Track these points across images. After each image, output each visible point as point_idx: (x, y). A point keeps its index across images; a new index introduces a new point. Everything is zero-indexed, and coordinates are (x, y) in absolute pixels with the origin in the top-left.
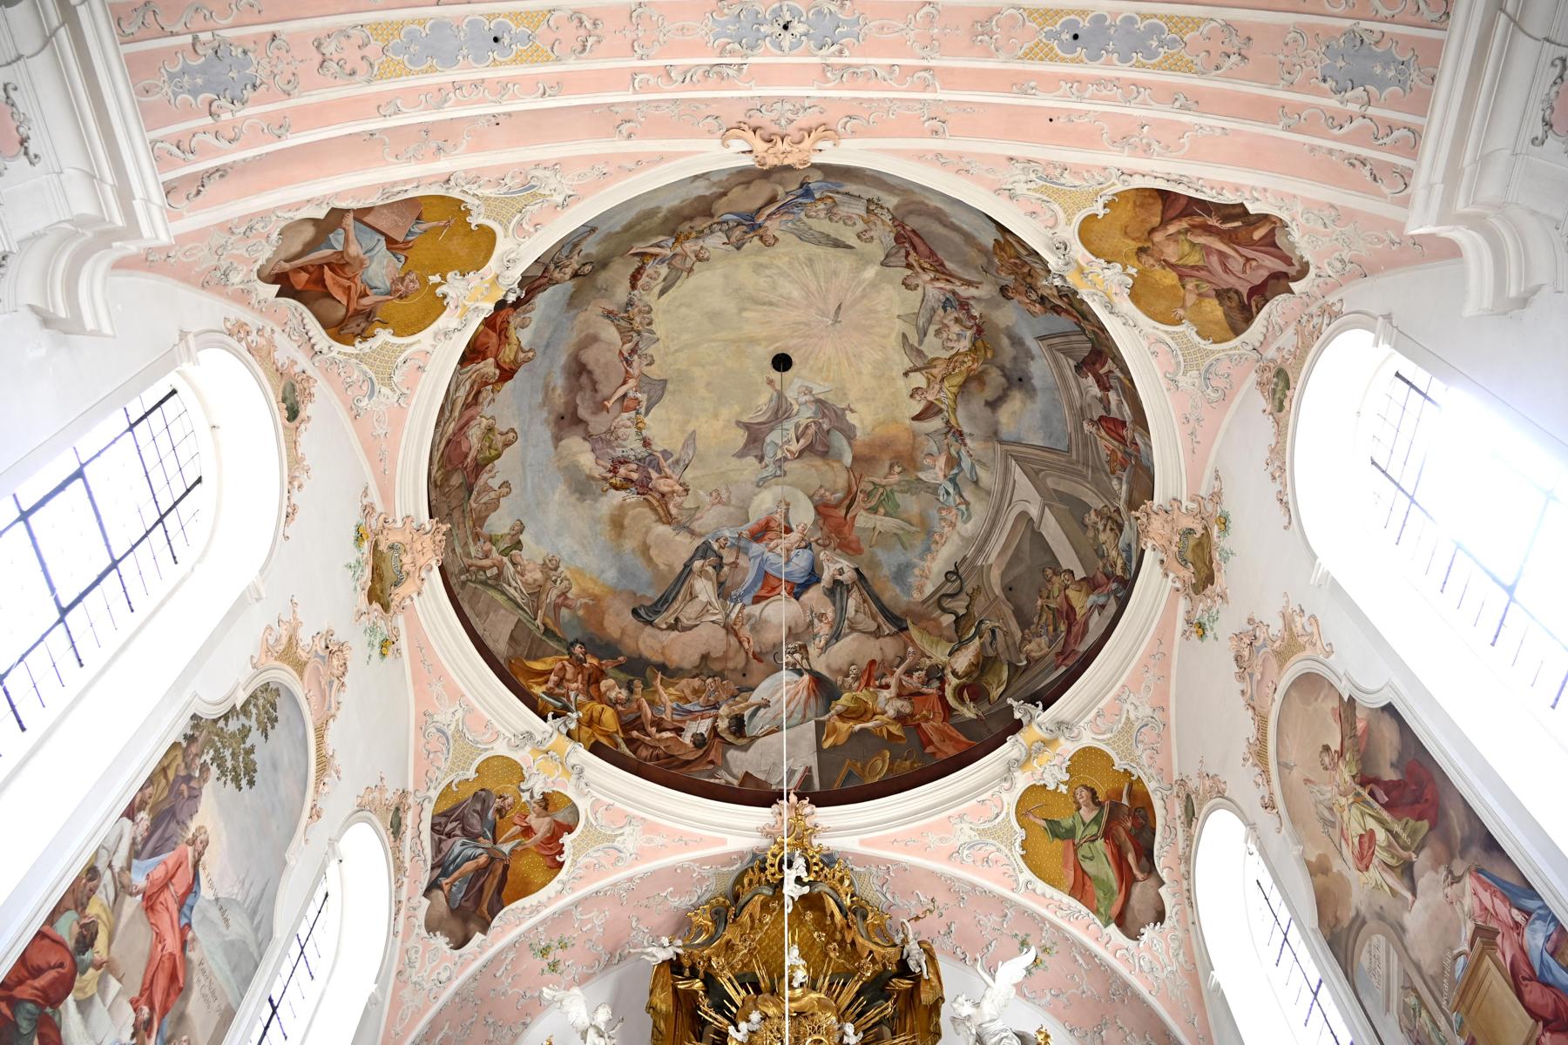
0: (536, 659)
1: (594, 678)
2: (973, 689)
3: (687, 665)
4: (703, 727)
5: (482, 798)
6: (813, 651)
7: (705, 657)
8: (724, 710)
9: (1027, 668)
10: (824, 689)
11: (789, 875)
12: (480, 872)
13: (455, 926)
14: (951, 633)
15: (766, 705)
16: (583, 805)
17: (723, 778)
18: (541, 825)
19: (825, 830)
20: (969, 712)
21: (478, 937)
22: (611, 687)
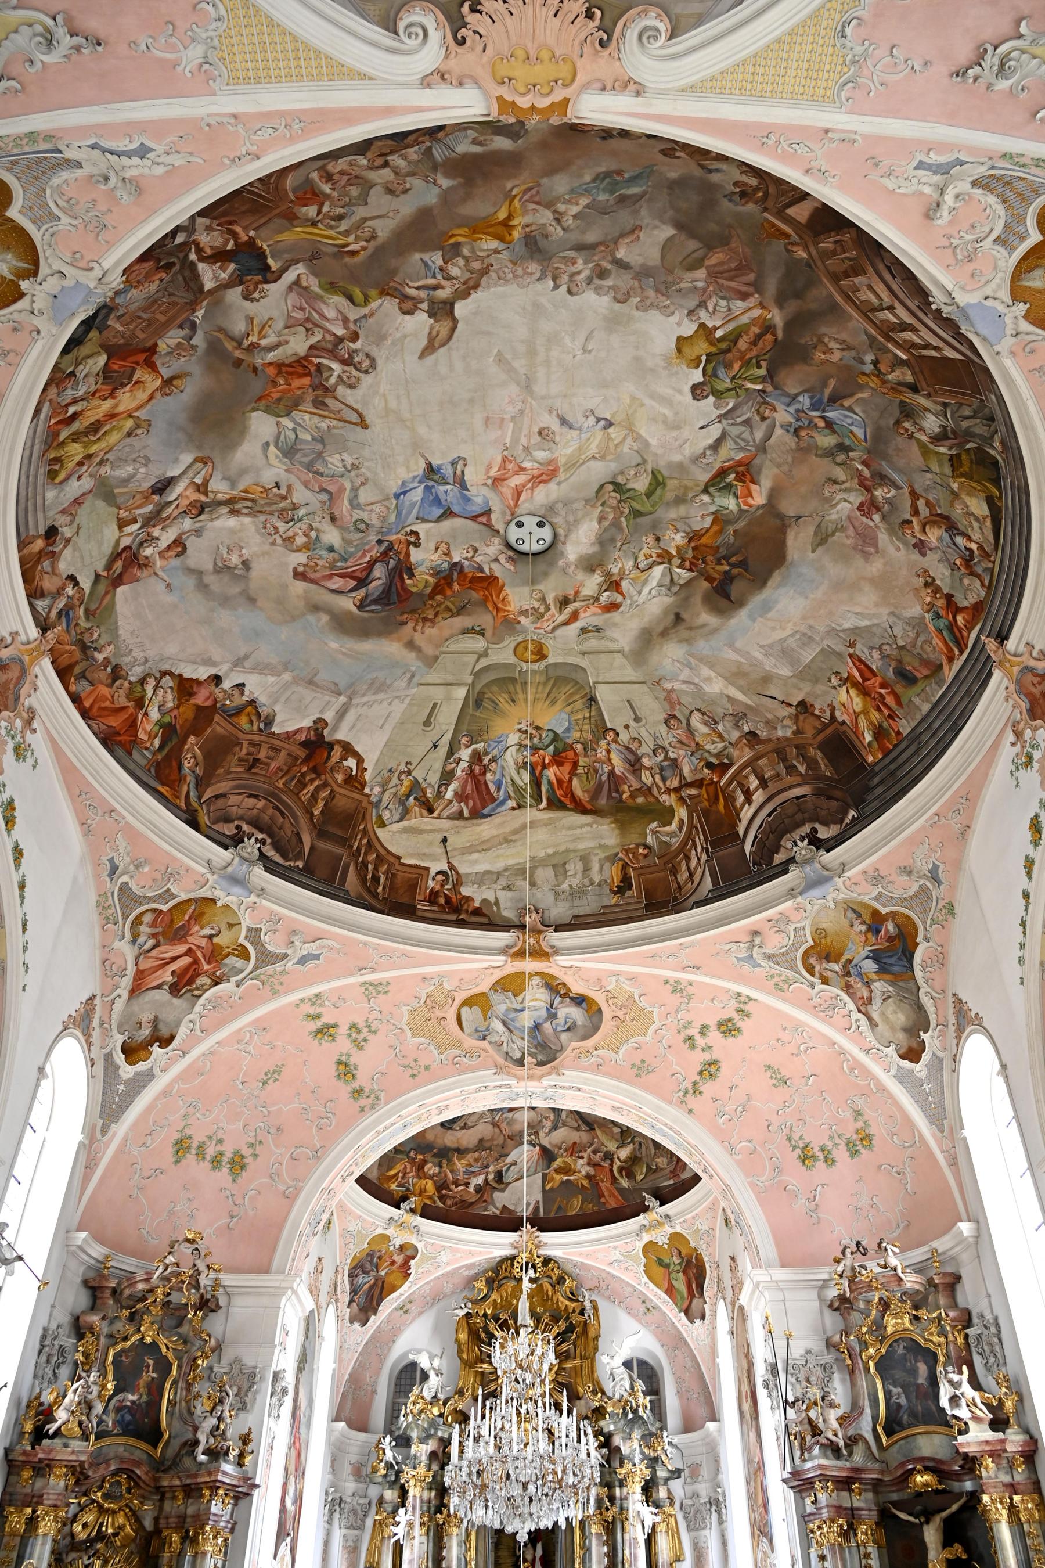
0: (390, 1169)
1: (421, 1167)
2: (628, 1170)
3: (471, 1146)
4: (480, 1180)
5: (371, 1255)
6: (542, 1134)
7: (481, 1141)
8: (491, 1168)
9: (655, 1171)
10: (547, 1155)
11: (526, 1279)
12: (371, 1287)
13: (362, 1317)
14: (618, 1137)
15: (515, 1163)
16: (420, 1246)
17: (493, 1211)
18: (399, 1259)
19: (546, 1245)
20: (625, 1183)
21: (373, 1317)
22: (431, 1169)
